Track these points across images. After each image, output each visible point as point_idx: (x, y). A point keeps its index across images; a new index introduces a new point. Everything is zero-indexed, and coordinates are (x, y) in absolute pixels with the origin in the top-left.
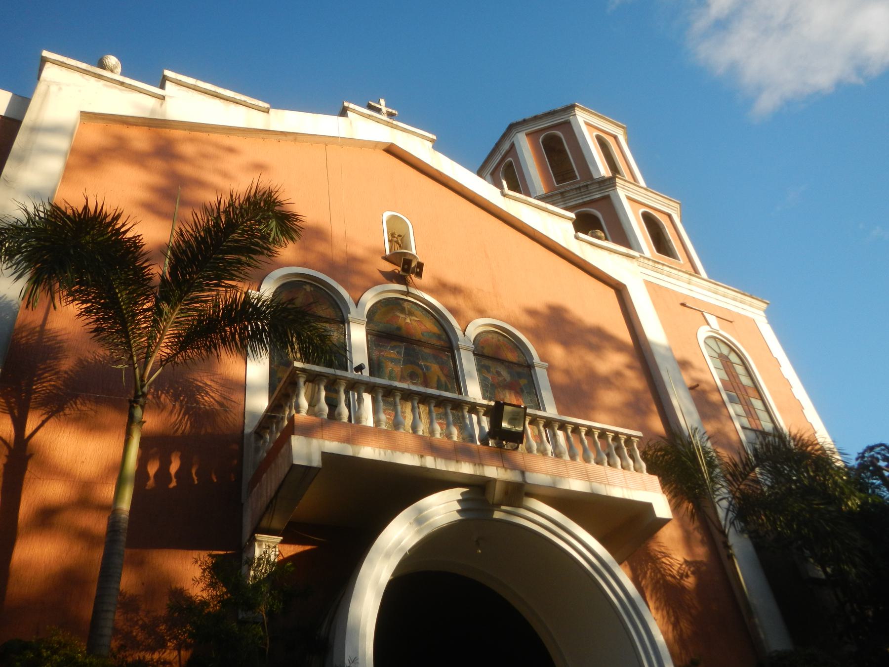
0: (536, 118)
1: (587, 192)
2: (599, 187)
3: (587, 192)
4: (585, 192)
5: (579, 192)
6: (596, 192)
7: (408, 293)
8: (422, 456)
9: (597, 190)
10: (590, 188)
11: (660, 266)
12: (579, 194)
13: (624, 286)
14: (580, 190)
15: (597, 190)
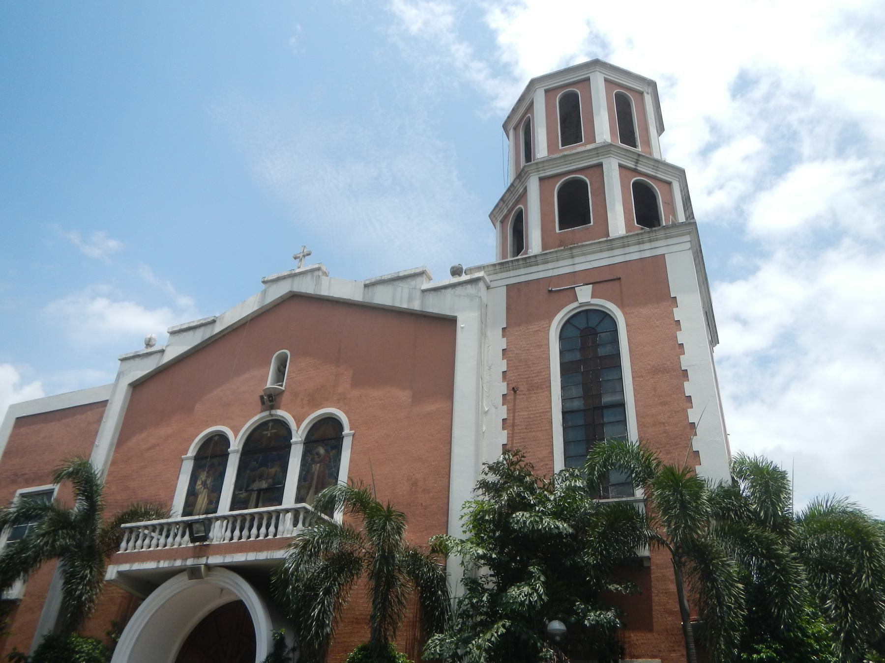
0: (514, 110)
1: (515, 190)
2: (520, 181)
3: (515, 190)
4: (514, 190)
5: (510, 192)
6: (520, 186)
7: (271, 415)
8: (159, 562)
9: (520, 184)
10: (515, 185)
11: (533, 260)
12: (512, 195)
13: (456, 317)
14: (510, 190)
15: (520, 184)
